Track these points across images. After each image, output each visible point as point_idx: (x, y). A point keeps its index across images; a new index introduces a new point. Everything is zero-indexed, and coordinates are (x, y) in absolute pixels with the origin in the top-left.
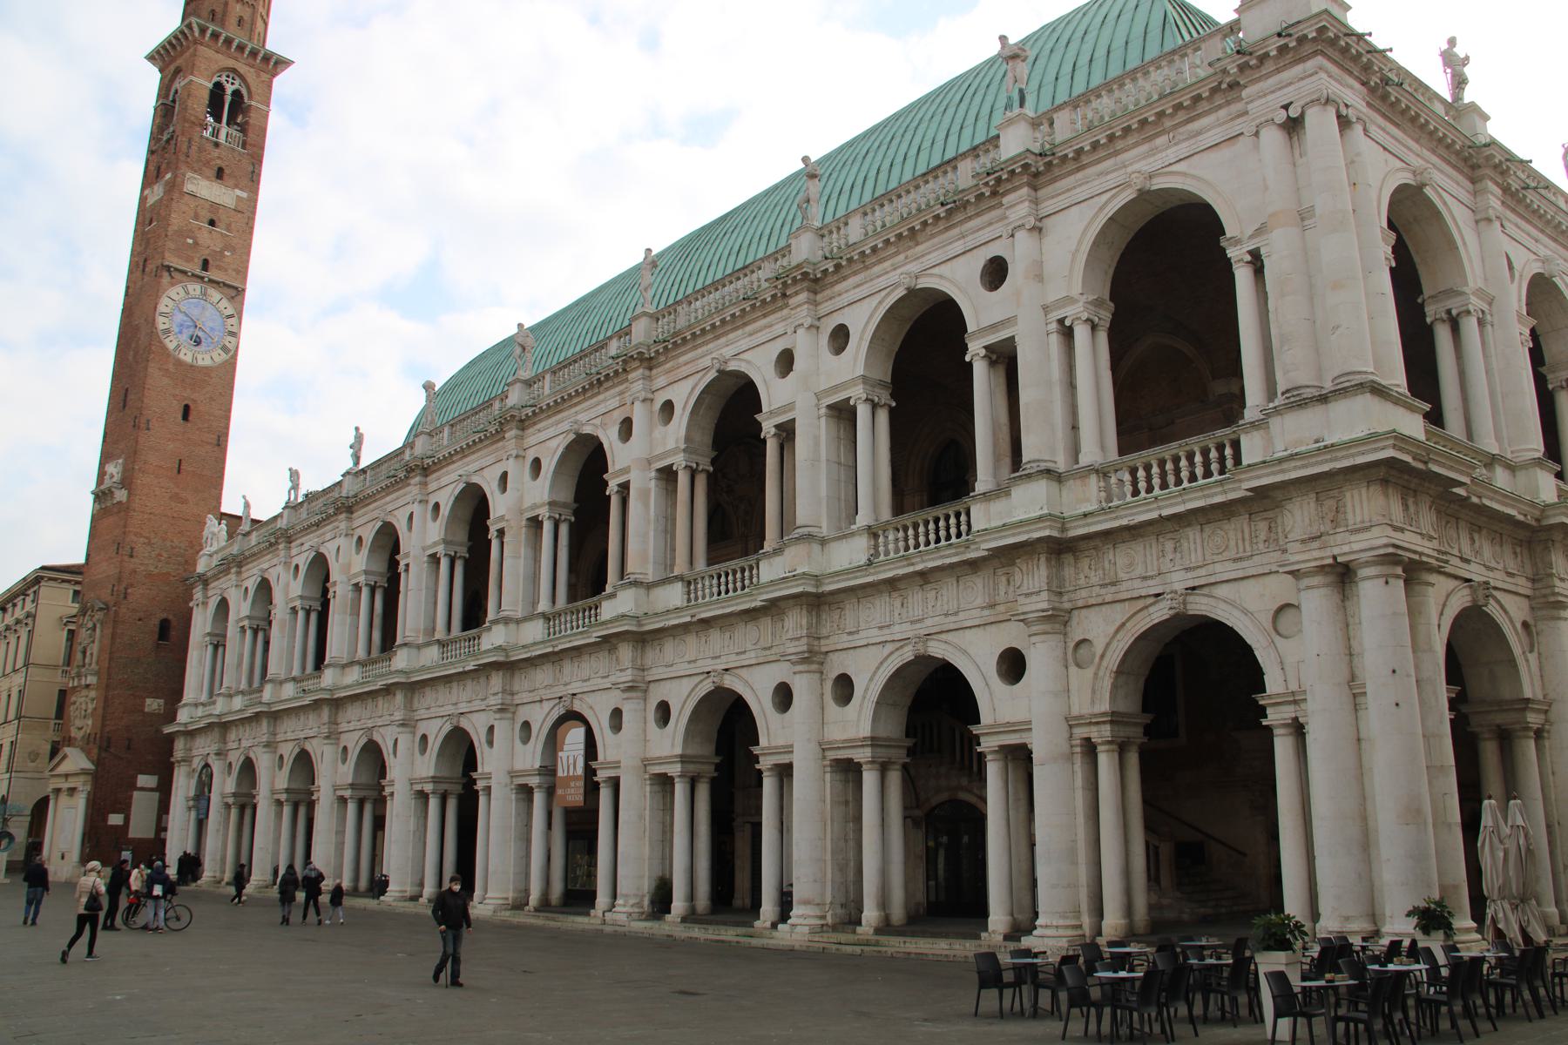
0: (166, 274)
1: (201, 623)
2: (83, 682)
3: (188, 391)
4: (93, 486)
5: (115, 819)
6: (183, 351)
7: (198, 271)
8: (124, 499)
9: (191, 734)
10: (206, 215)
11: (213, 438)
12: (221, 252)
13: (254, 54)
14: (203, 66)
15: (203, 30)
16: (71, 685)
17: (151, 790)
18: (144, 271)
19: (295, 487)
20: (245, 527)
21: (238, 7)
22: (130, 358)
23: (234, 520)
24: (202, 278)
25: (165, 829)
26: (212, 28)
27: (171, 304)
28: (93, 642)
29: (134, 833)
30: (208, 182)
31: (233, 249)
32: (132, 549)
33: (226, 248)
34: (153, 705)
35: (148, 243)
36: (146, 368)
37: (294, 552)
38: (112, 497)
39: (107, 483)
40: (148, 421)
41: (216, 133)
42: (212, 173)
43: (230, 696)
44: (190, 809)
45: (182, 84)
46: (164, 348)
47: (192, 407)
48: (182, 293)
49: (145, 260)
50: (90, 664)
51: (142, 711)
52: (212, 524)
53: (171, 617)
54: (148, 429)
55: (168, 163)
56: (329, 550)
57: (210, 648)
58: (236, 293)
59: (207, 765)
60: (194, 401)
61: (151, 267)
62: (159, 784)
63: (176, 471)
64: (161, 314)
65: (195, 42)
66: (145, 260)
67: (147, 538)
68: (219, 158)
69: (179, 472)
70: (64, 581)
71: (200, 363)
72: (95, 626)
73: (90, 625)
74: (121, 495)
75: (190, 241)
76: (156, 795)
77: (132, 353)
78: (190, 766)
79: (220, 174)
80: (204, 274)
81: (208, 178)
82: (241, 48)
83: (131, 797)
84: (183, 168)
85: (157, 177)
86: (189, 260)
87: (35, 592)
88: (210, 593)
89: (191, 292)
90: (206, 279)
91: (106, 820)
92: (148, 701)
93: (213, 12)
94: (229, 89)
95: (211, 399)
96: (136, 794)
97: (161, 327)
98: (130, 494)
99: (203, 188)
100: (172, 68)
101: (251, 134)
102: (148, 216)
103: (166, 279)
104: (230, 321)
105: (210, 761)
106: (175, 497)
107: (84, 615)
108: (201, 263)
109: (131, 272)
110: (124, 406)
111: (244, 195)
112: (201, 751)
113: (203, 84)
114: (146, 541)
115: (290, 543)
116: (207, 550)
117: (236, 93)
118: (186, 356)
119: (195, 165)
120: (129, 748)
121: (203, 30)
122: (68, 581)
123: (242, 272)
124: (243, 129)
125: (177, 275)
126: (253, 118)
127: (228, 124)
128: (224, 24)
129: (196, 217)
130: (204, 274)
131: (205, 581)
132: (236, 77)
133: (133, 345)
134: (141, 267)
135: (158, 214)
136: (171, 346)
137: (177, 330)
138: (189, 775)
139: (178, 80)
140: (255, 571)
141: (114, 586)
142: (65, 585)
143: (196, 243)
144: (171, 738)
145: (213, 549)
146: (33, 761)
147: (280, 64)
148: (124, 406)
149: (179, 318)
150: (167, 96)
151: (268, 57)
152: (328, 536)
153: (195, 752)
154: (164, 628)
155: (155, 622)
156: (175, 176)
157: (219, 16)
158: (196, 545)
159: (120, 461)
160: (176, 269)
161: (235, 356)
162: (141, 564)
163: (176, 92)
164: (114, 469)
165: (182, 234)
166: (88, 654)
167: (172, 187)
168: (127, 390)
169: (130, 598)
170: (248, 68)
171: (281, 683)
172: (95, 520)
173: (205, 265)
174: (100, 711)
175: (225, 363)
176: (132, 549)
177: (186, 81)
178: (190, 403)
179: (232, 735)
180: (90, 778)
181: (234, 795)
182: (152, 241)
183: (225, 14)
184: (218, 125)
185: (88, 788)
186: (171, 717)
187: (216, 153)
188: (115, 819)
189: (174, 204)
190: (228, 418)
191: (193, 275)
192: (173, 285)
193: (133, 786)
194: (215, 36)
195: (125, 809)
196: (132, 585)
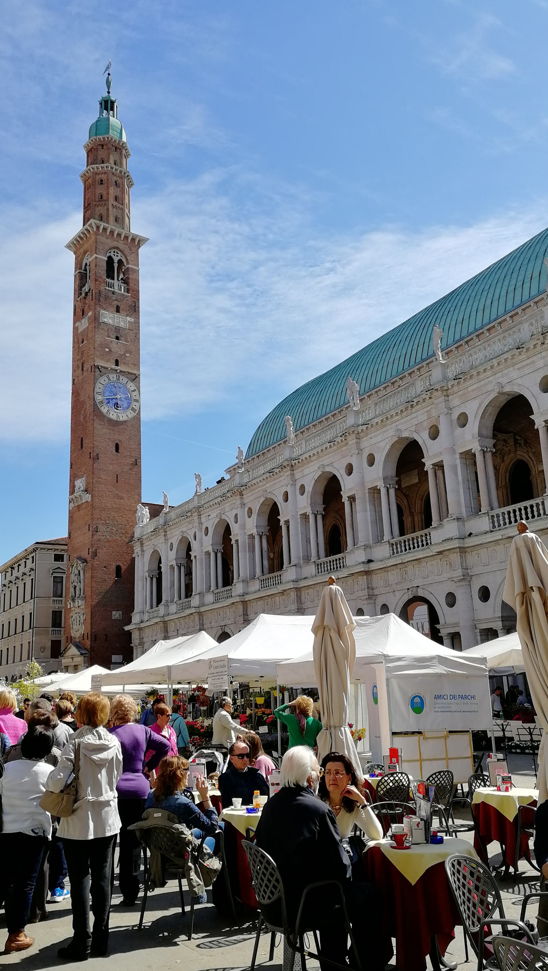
6: (112, 413)
8: (89, 500)
12: (125, 354)
13: (126, 238)
14: (101, 248)
15: (98, 228)
18: (82, 370)
20: (166, 510)
22: (82, 419)
26: (103, 225)
31: (130, 352)
32: (97, 527)
33: (127, 351)
34: (116, 615)
35: (83, 353)
37: (203, 520)
41: (112, 286)
46: (101, 412)
47: (119, 444)
48: (107, 380)
53: (121, 565)
55: (89, 306)
58: (135, 378)
60: (120, 441)
68: (116, 300)
71: (121, 419)
72: (79, 572)
75: (108, 350)
79: (118, 310)
81: (112, 312)
82: (119, 235)
85: (83, 315)
87: (33, 557)
89: (112, 379)
90: (118, 371)
94: (116, 259)
98: (92, 496)
100: (82, 251)
107: (72, 567)
108: (114, 362)
109: (74, 371)
110: (82, 447)
111: (133, 320)
114: (104, 522)
117: (120, 262)
118: (113, 415)
119: (104, 306)
120: (106, 640)
121: (98, 228)
123: (137, 365)
127: (118, 280)
128: (108, 222)
129: (109, 337)
132: (119, 252)
133: (82, 412)
134: (81, 367)
137: (107, 401)
139: (86, 257)
141: (89, 549)
142: (50, 552)
143: (110, 350)
146: (42, 652)
148: (82, 447)
150: (81, 268)
152: (227, 510)
155: (114, 567)
157: (104, 217)
161: (139, 413)
162: (103, 536)
163: (86, 264)
164: (80, 484)
165: (103, 346)
168: (82, 439)
170: (124, 246)
174: (89, 621)
178: (118, 442)
180: (86, 659)
184: (113, 281)
186: (129, 622)
192: (101, 376)
194: (105, 229)
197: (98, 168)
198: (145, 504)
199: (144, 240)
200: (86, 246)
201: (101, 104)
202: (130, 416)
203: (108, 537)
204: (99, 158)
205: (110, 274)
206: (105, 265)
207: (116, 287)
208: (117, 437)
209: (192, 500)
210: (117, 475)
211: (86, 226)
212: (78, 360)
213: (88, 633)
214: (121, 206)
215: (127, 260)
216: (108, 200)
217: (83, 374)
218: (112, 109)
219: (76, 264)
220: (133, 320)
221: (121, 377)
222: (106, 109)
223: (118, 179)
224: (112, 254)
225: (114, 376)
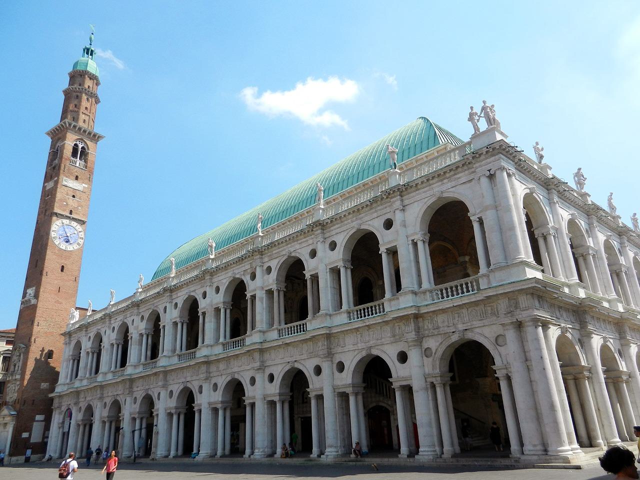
2: (14, 378)
3: (63, 260)
5: (25, 435)
9: (60, 397)
15: (70, 125)
16: (8, 379)
18: (45, 214)
24: (70, 217)
25: (48, 437)
26: (74, 123)
28: (19, 361)
29: (32, 441)
31: (82, 206)
32: (38, 323)
34: (44, 385)
36: (46, 252)
37: (112, 322)
38: (30, 302)
43: (82, 380)
44: (60, 428)
45: (61, 144)
49: (46, 210)
50: (18, 370)
51: (39, 388)
54: (47, 275)
57: (71, 361)
59: (69, 409)
62: (44, 419)
64: (53, 231)
66: (46, 210)
67: (45, 318)
71: (69, 249)
72: (20, 354)
74: (33, 301)
75: (65, 203)
77: (40, 246)
78: (61, 409)
79: (77, 178)
80: (69, 215)
84: (61, 176)
86: (64, 210)
88: (72, 339)
91: (21, 435)
94: (80, 146)
97: (53, 236)
100: (56, 138)
101: (88, 163)
102: (47, 194)
106: (57, 302)
109: (39, 215)
111: (86, 186)
112: (66, 403)
114: (45, 319)
115: (111, 318)
117: (83, 148)
118: (63, 246)
120: (33, 404)
121: (70, 125)
122: (4, 337)
124: (86, 162)
126: (90, 158)
129: (67, 195)
135: (52, 193)
136: (57, 243)
138: (60, 413)
139: (59, 142)
143: (67, 204)
144: (52, 400)
145: (74, 321)
148: (36, 267)
149: (61, 232)
150: (54, 148)
151: (95, 135)
152: (128, 316)
153: (63, 404)
156: (58, 178)
159: (34, 288)
160: (59, 214)
164: (31, 291)
165: (61, 200)
166: (17, 366)
167: (57, 183)
168: (37, 260)
171: (106, 374)
172: (21, 312)
173: (71, 212)
175: (78, 249)
176: (38, 323)
177: (63, 143)
179: (82, 396)
180: (15, 418)
182: (49, 203)
186: (52, 390)
187: (76, 169)
188: (25, 435)
189: (58, 190)
191: (66, 216)
193: (34, 420)
195: (29, 430)
196: (38, 337)
197: (75, 88)
198: (77, 308)
199: (101, 137)
200: (60, 135)
201: (84, 50)
202: (75, 248)
205: (74, 154)
206: (72, 149)
207: (77, 165)
211: (62, 123)
212: (43, 208)
213: (19, 399)
214: (88, 114)
217: (44, 218)
220: (86, 186)
221: (73, 222)
222: (87, 53)
224: (78, 142)
225: (68, 221)
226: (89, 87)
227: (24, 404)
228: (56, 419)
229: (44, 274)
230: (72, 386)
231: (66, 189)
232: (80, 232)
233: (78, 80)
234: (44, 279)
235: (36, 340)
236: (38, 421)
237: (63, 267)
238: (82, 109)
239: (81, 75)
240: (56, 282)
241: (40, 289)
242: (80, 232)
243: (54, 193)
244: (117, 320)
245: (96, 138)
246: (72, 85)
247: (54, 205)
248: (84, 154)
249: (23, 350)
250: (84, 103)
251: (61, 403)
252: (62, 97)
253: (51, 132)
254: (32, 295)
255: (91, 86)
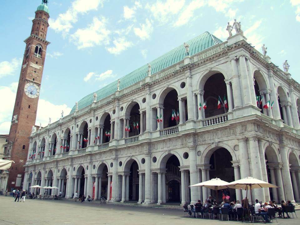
0: (26, 81)
1: (31, 146)
2: (8, 157)
4: (11, 120)
5: (13, 183)
7: (32, 81)
9: (28, 167)
10: (34, 70)
11: (34, 111)
13: (44, 41)
15: (34, 37)
17: (20, 177)
18: (22, 80)
19: (50, 121)
20: (40, 128)
21: (41, 33)
23: (38, 127)
24: (33, 82)
25: (23, 185)
26: (36, 36)
27: (27, 86)
29: (17, 185)
30: (34, 64)
31: (39, 77)
34: (22, 161)
36: (22, 98)
37: (50, 133)
39: (14, 119)
40: (22, 108)
41: (36, 55)
42: (36, 63)
43: (36, 160)
46: (25, 94)
49: (22, 78)
52: (35, 129)
53: (24, 144)
56: (57, 133)
57: (33, 151)
58: (39, 85)
59: (31, 173)
60: (31, 105)
61: (23, 80)
63: (27, 118)
64: (26, 88)
65: (33, 39)
66: (22, 78)
69: (28, 117)
70: (4, 138)
71: (32, 98)
73: (10, 146)
74: (16, 122)
75: (31, 75)
76: (21, 178)
79: (37, 63)
80: (33, 81)
81: (34, 63)
82: (41, 40)
83: (16, 179)
84: (30, 62)
86: (31, 79)
91: (11, 183)
92: (20, 160)
93: (36, 34)
94: (39, 47)
95: (34, 104)
96: (17, 178)
98: (18, 122)
99: (33, 65)
100: (28, 43)
103: (26, 82)
104: (38, 90)
105: (32, 172)
108: (33, 79)
109: (20, 80)
111: (41, 67)
113: (34, 46)
116: (33, 132)
117: (40, 48)
118: (30, 96)
121: (34, 37)
123: (40, 81)
124: (41, 55)
125: (28, 81)
126: (43, 53)
129: (32, 71)
130: (33, 81)
131: (32, 138)
138: (28, 175)
140: (42, 136)
142: (4, 138)
143: (32, 76)
145: (34, 132)
147: (48, 43)
149: (29, 89)
151: (46, 42)
152: (57, 130)
153: (29, 170)
154: (24, 147)
155: (22, 146)
156: (28, 63)
157: (37, 34)
158: (30, 131)
159: (17, 115)
160: (28, 80)
161: (38, 97)
163: (29, 48)
164: (15, 117)
165: (29, 74)
167: (28, 65)
169: (18, 141)
171: (47, 157)
172: (11, 126)
173: (34, 80)
179: (37, 167)
180: (8, 175)
181: (37, 178)
183: (39, 34)
185: (8, 177)
186: (25, 164)
187: (36, 59)
188: (13, 183)
189: (28, 68)
190: (37, 108)
191: (32, 81)
192: (27, 83)
193: (17, 177)
194: (37, 38)
195: (15, 181)
196: (18, 139)
198: (35, 126)
202: (36, 97)
203: (22, 135)
204: (39, 16)
205: (36, 51)
207: (37, 57)
208: (30, 103)
209: (47, 126)
210: (28, 116)
215: (43, 48)
216: (39, 29)
218: (46, 3)
219: (26, 47)
221: (34, 84)
222: (44, 2)
223: (44, 23)
224: (38, 46)
226: (44, 18)
227: (12, 169)
228: (26, 177)
229: (21, 109)
230: (32, 162)
231: (32, 68)
232: (38, 89)
233: (40, 15)
234: (21, 111)
235: (18, 140)
236: (18, 177)
237: (29, 106)
238: (41, 30)
239: (41, 13)
240: (26, 113)
241: (19, 116)
242: (38, 89)
243: (26, 70)
244: (52, 132)
245: (47, 43)
246: (37, 17)
247: (26, 76)
248: (41, 51)
249: (12, 144)
250: (42, 27)
251: (28, 170)
252: (32, 23)
253: (26, 40)
254: (16, 118)
255: (45, 18)
